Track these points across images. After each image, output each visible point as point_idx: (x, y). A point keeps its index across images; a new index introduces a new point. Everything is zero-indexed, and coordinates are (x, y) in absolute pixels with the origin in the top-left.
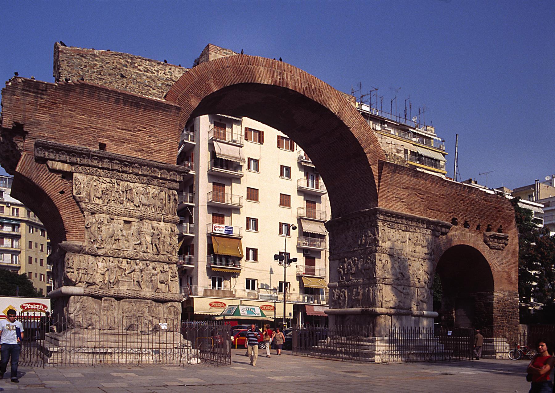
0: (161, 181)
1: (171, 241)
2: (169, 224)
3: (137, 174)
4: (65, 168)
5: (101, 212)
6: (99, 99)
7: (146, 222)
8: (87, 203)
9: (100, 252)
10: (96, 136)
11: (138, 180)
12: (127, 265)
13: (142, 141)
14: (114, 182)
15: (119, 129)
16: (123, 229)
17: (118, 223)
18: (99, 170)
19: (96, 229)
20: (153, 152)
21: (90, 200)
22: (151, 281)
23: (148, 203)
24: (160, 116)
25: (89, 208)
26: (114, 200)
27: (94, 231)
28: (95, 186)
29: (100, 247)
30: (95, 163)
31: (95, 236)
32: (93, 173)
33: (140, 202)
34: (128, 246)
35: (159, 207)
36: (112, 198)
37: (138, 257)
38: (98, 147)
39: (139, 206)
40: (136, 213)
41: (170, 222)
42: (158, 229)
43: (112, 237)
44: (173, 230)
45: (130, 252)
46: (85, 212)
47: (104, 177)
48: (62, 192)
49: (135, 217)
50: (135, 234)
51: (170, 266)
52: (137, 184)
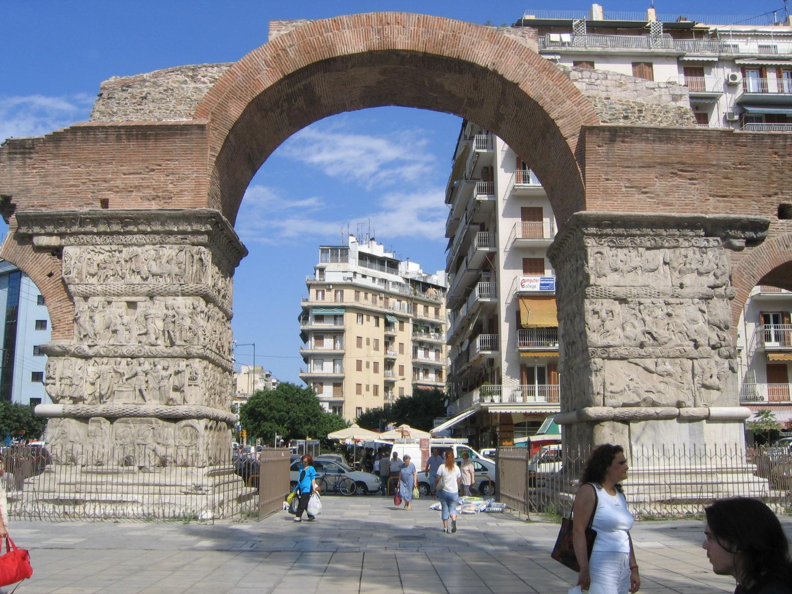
0: (180, 236)
2: (191, 298)
3: (145, 233)
4: (53, 241)
5: (95, 294)
6: (96, 142)
7: (160, 301)
8: (78, 284)
9: (91, 352)
10: (96, 191)
11: (148, 241)
12: (126, 367)
13: (156, 184)
14: (113, 249)
15: (125, 174)
16: (123, 314)
17: (119, 307)
19: (88, 318)
20: (172, 195)
21: (81, 280)
22: (159, 388)
24: (178, 143)
25: (79, 291)
26: (113, 275)
27: (85, 321)
28: (89, 259)
29: (92, 344)
30: (89, 228)
31: (85, 330)
32: (87, 242)
33: (150, 271)
34: (130, 339)
36: (111, 273)
38: (99, 204)
39: (147, 279)
40: (142, 289)
45: (132, 346)
46: (74, 298)
47: (101, 245)
48: (50, 275)
49: (142, 294)
51: (190, 361)
52: (147, 247)
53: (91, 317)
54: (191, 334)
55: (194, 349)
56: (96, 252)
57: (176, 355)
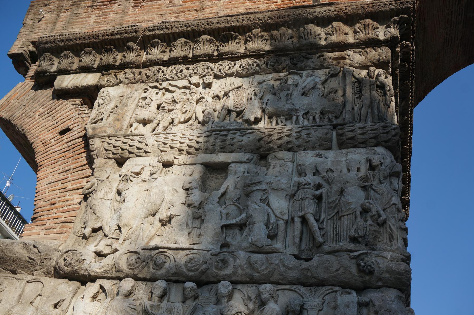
1: (367, 197)
2: (361, 150)
8: (109, 137)
18: (164, 68)
23: (287, 107)
25: (110, 147)
35: (322, 113)
37: (228, 271)
40: (245, 138)
41: (365, 144)
42: (316, 173)
43: (154, 215)
44: (375, 163)
47: (173, 79)
49: (241, 149)
50: (233, 194)
51: (373, 295)
53: (119, 193)
54: (370, 222)
55: (380, 260)
56: (160, 89)
57: (326, 276)
